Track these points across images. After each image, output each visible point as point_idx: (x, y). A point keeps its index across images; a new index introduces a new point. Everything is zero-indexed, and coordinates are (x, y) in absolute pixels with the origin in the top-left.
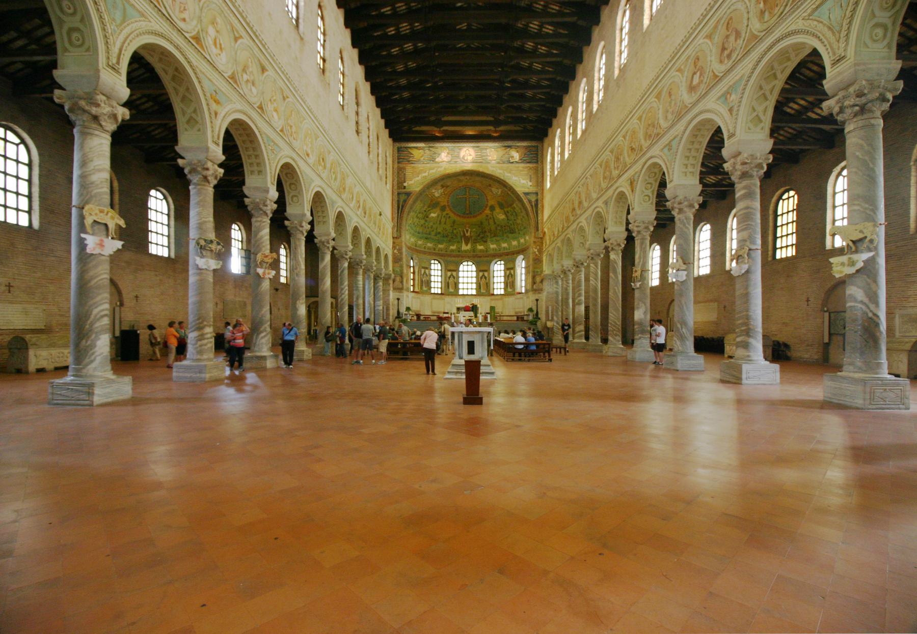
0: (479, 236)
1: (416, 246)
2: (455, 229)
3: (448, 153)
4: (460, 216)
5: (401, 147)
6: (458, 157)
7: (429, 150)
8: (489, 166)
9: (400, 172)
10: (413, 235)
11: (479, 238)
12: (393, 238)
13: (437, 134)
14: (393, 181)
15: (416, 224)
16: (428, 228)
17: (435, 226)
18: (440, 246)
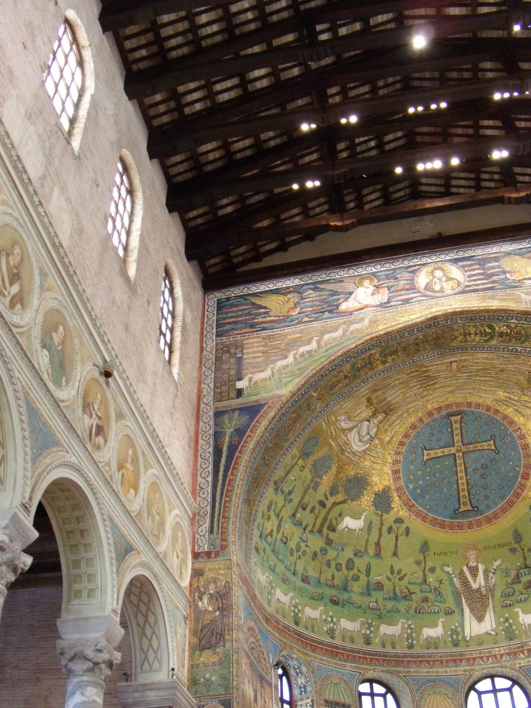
0: (517, 579)
1: (297, 624)
2: (433, 570)
3: (377, 287)
4: (442, 525)
5: (228, 299)
6: (413, 288)
7: (315, 289)
8: (517, 292)
9: (226, 356)
10: (285, 581)
11: (519, 587)
12: (196, 556)
13: (332, 224)
14: (200, 384)
15: (292, 544)
16: (338, 567)
17: (360, 563)
18: (385, 629)
